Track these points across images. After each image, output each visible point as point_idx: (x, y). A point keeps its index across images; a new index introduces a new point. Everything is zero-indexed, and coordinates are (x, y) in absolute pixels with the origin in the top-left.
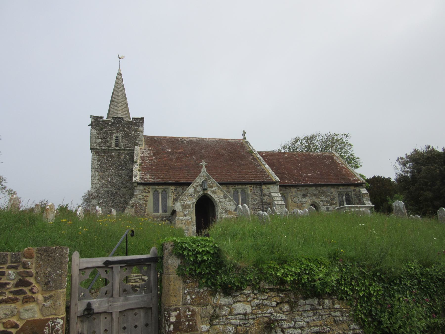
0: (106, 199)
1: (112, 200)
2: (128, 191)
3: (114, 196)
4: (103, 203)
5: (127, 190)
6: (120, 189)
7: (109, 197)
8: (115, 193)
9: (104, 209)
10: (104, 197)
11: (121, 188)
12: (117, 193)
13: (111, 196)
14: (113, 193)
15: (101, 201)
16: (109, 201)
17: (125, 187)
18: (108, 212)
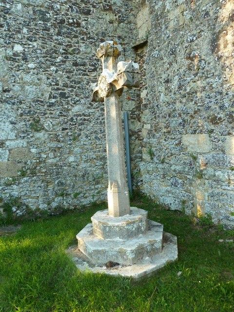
0: (40, 42)
1: (61, 50)
2: (116, 24)
3: (68, 35)
4: (25, 59)
5: (111, 22)
6: (88, 13)
7: (50, 37)
8: (70, 24)
9: (32, 83)
10: (30, 30)
11: (94, 7)
12: (79, 25)
13: (59, 34)
14: (62, 21)
15: (18, 48)
16: (51, 54)
17: (105, 10)
18: (50, 97)
